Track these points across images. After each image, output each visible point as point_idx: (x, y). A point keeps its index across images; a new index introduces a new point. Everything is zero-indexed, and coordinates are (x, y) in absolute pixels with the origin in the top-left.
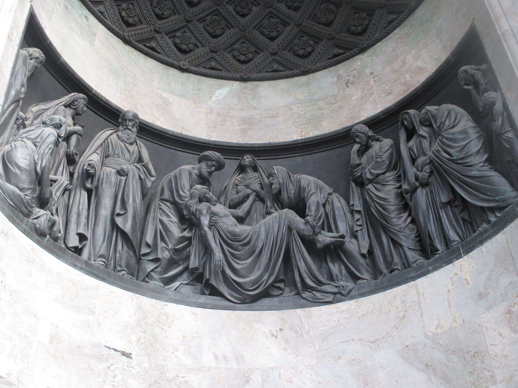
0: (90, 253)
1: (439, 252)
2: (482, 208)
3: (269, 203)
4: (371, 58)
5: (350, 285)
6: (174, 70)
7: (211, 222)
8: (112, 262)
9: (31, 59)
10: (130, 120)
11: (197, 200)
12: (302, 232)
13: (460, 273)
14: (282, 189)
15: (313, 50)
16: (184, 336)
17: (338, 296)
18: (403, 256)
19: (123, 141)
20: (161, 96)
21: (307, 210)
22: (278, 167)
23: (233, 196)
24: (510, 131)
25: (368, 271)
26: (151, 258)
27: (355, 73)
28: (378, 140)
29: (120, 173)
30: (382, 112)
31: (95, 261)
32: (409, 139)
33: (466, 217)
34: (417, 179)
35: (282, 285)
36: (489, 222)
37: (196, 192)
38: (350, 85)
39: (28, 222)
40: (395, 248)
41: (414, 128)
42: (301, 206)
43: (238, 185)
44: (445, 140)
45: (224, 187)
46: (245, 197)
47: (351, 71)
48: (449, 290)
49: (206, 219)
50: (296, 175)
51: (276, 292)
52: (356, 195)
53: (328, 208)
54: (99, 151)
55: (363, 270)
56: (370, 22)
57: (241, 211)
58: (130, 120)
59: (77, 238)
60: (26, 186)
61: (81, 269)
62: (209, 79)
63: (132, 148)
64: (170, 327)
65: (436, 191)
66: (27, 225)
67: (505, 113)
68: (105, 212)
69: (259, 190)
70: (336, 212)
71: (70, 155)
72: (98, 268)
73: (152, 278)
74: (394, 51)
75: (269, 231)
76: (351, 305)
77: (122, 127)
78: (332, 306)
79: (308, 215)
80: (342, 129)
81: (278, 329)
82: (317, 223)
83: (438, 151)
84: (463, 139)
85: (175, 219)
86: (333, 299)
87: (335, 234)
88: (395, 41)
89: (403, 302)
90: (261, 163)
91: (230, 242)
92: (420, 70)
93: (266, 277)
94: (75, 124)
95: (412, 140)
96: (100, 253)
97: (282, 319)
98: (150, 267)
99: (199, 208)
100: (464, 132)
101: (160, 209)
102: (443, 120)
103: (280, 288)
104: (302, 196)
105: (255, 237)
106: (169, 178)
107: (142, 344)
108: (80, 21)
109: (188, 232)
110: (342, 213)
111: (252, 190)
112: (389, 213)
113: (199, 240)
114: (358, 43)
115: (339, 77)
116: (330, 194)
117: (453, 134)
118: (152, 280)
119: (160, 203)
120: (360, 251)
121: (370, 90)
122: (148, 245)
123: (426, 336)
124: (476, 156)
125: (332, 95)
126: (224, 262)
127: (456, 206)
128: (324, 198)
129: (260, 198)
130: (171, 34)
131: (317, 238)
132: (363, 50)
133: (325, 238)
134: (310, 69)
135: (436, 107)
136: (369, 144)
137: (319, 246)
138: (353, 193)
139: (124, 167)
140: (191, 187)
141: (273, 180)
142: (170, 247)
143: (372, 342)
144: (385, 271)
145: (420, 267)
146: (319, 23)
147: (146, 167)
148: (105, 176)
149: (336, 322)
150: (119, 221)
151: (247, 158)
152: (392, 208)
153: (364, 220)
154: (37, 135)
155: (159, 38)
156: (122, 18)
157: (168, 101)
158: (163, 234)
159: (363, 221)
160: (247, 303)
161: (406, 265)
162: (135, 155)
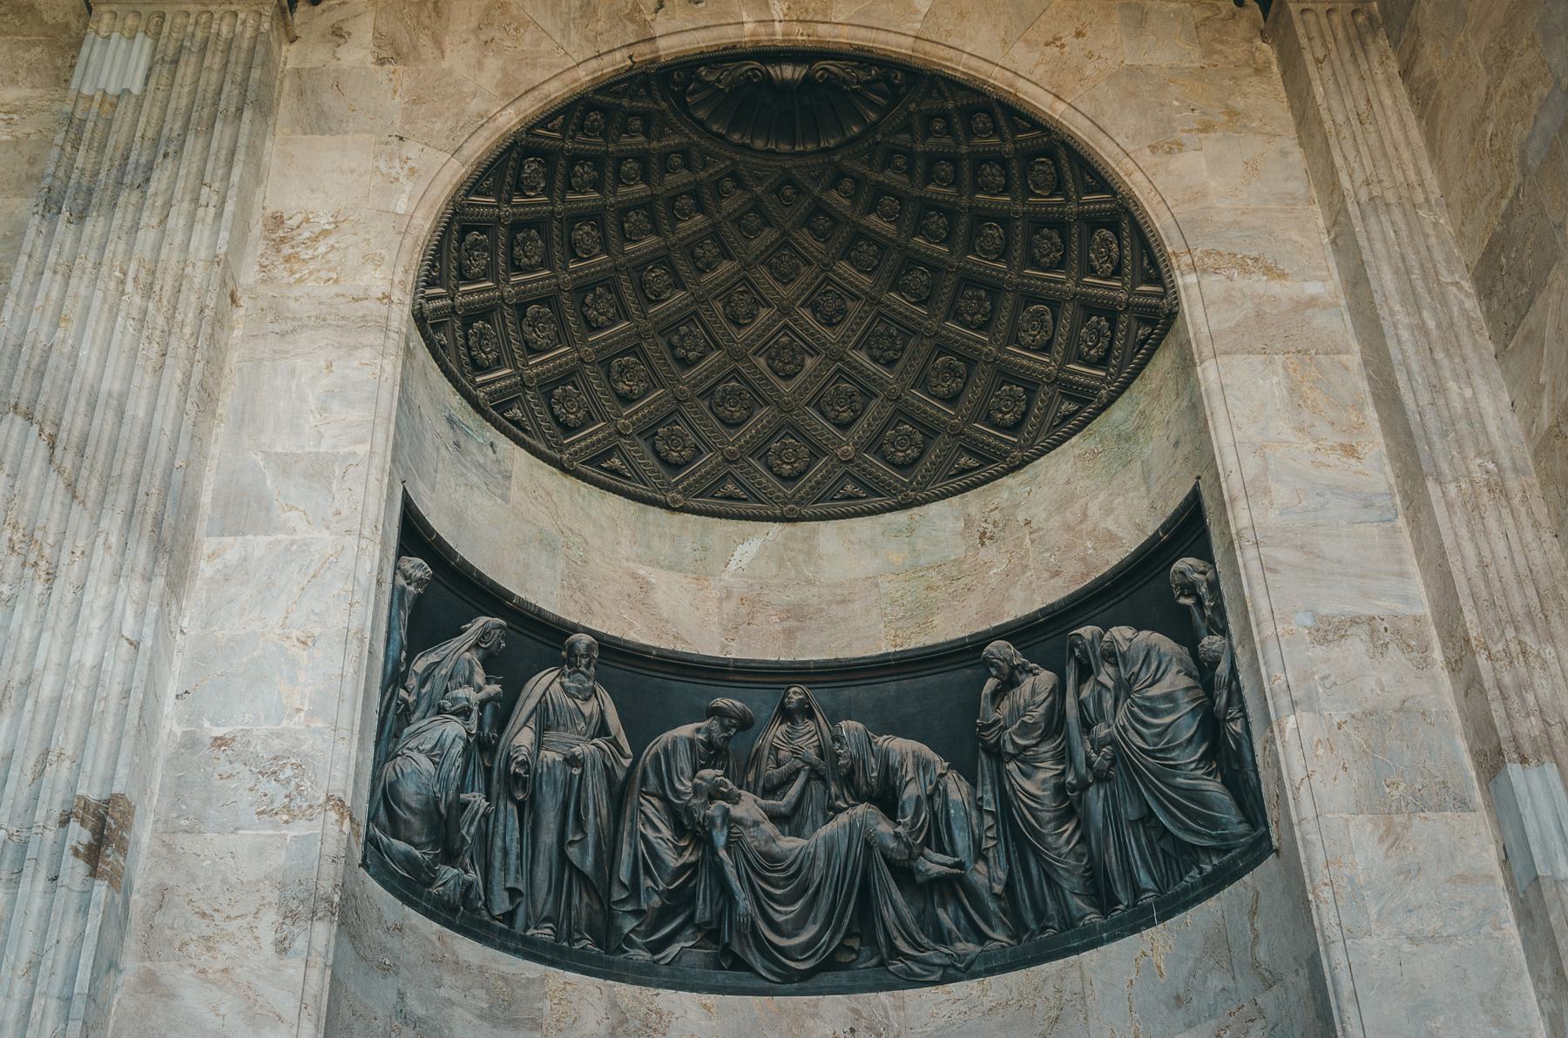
0: (527, 917)
3: (833, 789)
5: (970, 948)
6: (658, 510)
15: (922, 453)
17: (951, 971)
19: (571, 696)
20: (634, 576)
23: (771, 771)
26: (629, 908)
27: (996, 515)
29: (572, 761)
32: (1081, 680)
33: (1170, 850)
34: (1089, 763)
35: (855, 944)
36: (1201, 871)
44: (1135, 709)
51: (844, 958)
53: (938, 801)
54: (531, 724)
55: (995, 921)
56: (1029, 404)
57: (782, 804)
59: (506, 894)
61: (516, 952)
63: (589, 708)
66: (428, 901)
68: (548, 838)
72: (544, 943)
73: (632, 944)
74: (1068, 483)
81: (847, 1029)
83: (1124, 727)
84: (1169, 712)
85: (667, 833)
90: (819, 698)
93: (825, 938)
94: (488, 681)
98: (629, 924)
100: (1169, 697)
102: (1136, 669)
103: (852, 950)
108: (481, 460)
114: (1006, 452)
115: (969, 522)
116: (942, 775)
117: (1150, 699)
120: (991, 888)
129: (815, 774)
130: (647, 432)
132: (1013, 469)
133: (933, 864)
137: (919, 878)
139: (577, 750)
140: (695, 772)
144: (1033, 926)
150: (573, 852)
156: (556, 418)
157: (648, 582)
158: (649, 861)
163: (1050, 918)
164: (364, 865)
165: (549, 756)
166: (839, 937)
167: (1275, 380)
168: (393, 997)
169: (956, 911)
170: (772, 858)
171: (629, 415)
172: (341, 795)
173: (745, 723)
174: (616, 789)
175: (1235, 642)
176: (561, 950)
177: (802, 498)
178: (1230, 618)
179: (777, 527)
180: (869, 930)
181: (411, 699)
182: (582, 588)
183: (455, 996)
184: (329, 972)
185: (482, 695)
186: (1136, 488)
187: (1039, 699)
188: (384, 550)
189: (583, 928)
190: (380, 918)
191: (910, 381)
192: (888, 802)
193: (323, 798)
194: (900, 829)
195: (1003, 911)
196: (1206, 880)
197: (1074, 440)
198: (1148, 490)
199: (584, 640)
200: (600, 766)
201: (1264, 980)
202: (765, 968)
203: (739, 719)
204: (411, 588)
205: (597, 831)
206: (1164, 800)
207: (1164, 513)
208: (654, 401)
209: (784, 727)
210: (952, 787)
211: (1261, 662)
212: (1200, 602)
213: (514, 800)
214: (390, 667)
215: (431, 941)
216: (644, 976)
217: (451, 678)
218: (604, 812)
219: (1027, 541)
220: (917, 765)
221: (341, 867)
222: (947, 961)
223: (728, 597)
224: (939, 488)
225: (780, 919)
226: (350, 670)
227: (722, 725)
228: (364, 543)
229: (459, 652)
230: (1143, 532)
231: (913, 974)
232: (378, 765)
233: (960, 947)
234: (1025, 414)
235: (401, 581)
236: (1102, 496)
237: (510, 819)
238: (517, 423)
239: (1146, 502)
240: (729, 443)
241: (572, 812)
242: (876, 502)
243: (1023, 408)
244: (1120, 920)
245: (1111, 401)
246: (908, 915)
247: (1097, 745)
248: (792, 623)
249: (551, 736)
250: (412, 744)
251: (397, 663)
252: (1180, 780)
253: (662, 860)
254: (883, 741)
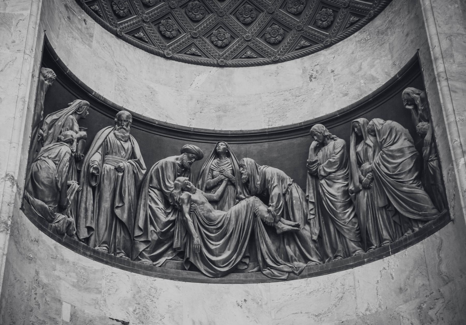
0: (95, 241)
1: (373, 247)
2: (410, 219)
3: (239, 189)
4: (333, 56)
5: (302, 265)
6: (159, 58)
8: (113, 246)
9: (46, 80)
10: (125, 121)
13: (387, 268)
14: (250, 180)
15: (283, 39)
16: (169, 306)
17: (292, 275)
18: (346, 245)
19: (119, 139)
20: (148, 87)
21: (270, 201)
22: (248, 159)
23: (209, 180)
24: (435, 160)
25: (317, 254)
26: (142, 239)
27: (318, 68)
28: (333, 138)
29: (118, 169)
30: (338, 111)
31: (99, 246)
32: (357, 143)
33: (397, 221)
34: (361, 181)
35: (247, 261)
36: (413, 231)
37: (180, 183)
38: (313, 80)
39: (51, 226)
40: (339, 237)
41: (362, 135)
42: (265, 194)
43: (213, 170)
44: (384, 155)
46: (219, 182)
47: (316, 65)
48: (378, 281)
52: (311, 188)
53: (288, 197)
54: (100, 151)
55: (313, 253)
57: (215, 195)
58: (125, 121)
59: (86, 230)
60: (50, 199)
62: (190, 65)
63: (127, 145)
64: (158, 299)
65: (375, 196)
66: (50, 229)
67: (433, 144)
68: (106, 205)
69: (231, 177)
70: (294, 201)
71: (78, 158)
72: (103, 254)
73: (143, 257)
74: (353, 53)
76: (302, 283)
77: (118, 126)
78: (287, 282)
79: (270, 205)
80: (304, 122)
82: (278, 213)
83: (378, 164)
84: (400, 157)
85: (161, 206)
86: (288, 277)
87: (292, 223)
88: (355, 43)
89: (343, 285)
90: (233, 148)
92: (373, 79)
93: (234, 257)
94: (80, 130)
95: (360, 145)
96: (104, 240)
97: (247, 292)
98: (142, 247)
99: (181, 197)
100: (401, 150)
101: (150, 195)
102: (385, 137)
103: (245, 264)
104: (267, 187)
107: (137, 314)
108: (80, 27)
110: (299, 203)
111: (225, 176)
112: (336, 209)
113: (181, 223)
114: (323, 39)
115: (304, 70)
116: (290, 185)
117: (391, 151)
118: (143, 258)
119: (150, 190)
120: (312, 237)
121: (329, 87)
122: (140, 229)
123: (358, 315)
124: (408, 174)
125: (297, 88)
126: (202, 244)
127: (390, 211)
128: (285, 188)
129: (230, 182)
130: (156, 22)
131: (277, 225)
132: (326, 47)
133: (285, 225)
134: (280, 59)
135: (381, 121)
136: (325, 142)
137: (278, 231)
138: (309, 185)
139: (121, 164)
140: (175, 178)
141: (243, 170)
142: (158, 231)
143: (316, 316)
144: (331, 255)
145: (359, 257)
146: (290, 13)
147: (138, 162)
148: (106, 172)
149: (289, 296)
151: (222, 145)
152: (339, 204)
153: (317, 210)
154: (55, 154)
155: (147, 28)
156: (114, 11)
157: (154, 91)
158: (152, 218)
159: (315, 211)
160: (219, 277)
161: (348, 254)
162: (129, 152)
163: (339, 252)
164: (22, 209)
165: (108, 167)
166: (240, 257)
167: (457, 6)
168: (33, 273)
169: (294, 247)
170: (210, 220)
171: (147, 14)
172: (13, 174)
173: (199, 157)
174: (138, 184)
175: (434, 124)
176: (111, 257)
177: (227, 56)
178: (432, 113)
179: (215, 69)
180: (258, 252)
181: (45, 135)
182: (124, 91)
183: (62, 275)
184: (5, 257)
185: (78, 136)
186: (386, 56)
187: (337, 151)
188: (35, 61)
189: (121, 248)
190: (29, 235)
191: (279, 5)
192: (265, 196)
193: (4, 175)
194: (270, 208)
195: (317, 248)
196: (416, 235)
197: (356, 34)
198: (392, 57)
199: (125, 114)
200: (131, 172)
201: (444, 280)
202: (205, 270)
203: (196, 154)
204: (46, 82)
205: (129, 202)
206: (397, 197)
207: (400, 67)
208: (159, 7)
209: (216, 161)
210: (294, 191)
211: (448, 133)
212: (416, 107)
213: (91, 186)
214: (36, 117)
215: (51, 249)
216: (148, 271)
217: (63, 127)
218: (133, 194)
219: (332, 79)
220: (279, 180)
221: (12, 208)
222: (290, 270)
223: (191, 100)
224: (290, 55)
225: (213, 247)
226: (18, 115)
228: (26, 56)
229: (67, 115)
230: (389, 75)
231: (275, 276)
232: (29, 164)
233: (296, 264)
234: (332, 22)
235: (42, 78)
236: (369, 59)
237: (89, 194)
238: (96, 12)
239: (391, 62)
240: (194, 29)
241: (117, 192)
242: (261, 60)
243: (332, 19)
244: (373, 253)
245: (375, 16)
246: (273, 248)
247: (365, 173)
248: (221, 113)
249: (109, 157)
250: (45, 155)
251: (39, 116)
252: (405, 189)
253: (159, 218)
254: (262, 168)
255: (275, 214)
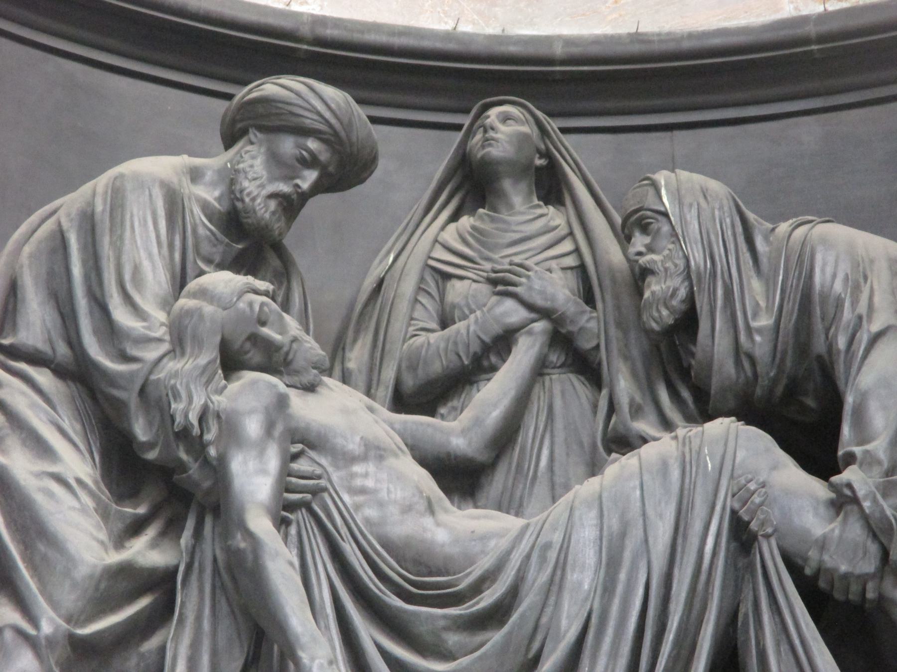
3: (625, 386)
7: (288, 491)
11: (209, 355)
12: (813, 554)
21: (846, 430)
22: (684, 175)
37: (208, 309)
42: (810, 402)
43: (447, 277)
45: (369, 283)
49: (264, 472)
50: (784, 227)
57: (461, 428)
75: (621, 548)
79: (850, 459)
85: (79, 465)
90: (585, 154)
91: (396, 602)
99: (220, 401)
104: (819, 346)
105: (538, 578)
106: (49, 225)
109: (154, 544)
111: (530, 307)
140: (180, 281)
141: (650, 249)
142: (46, 628)
151: (506, 118)
227: (274, 158)
255: (889, 512)
